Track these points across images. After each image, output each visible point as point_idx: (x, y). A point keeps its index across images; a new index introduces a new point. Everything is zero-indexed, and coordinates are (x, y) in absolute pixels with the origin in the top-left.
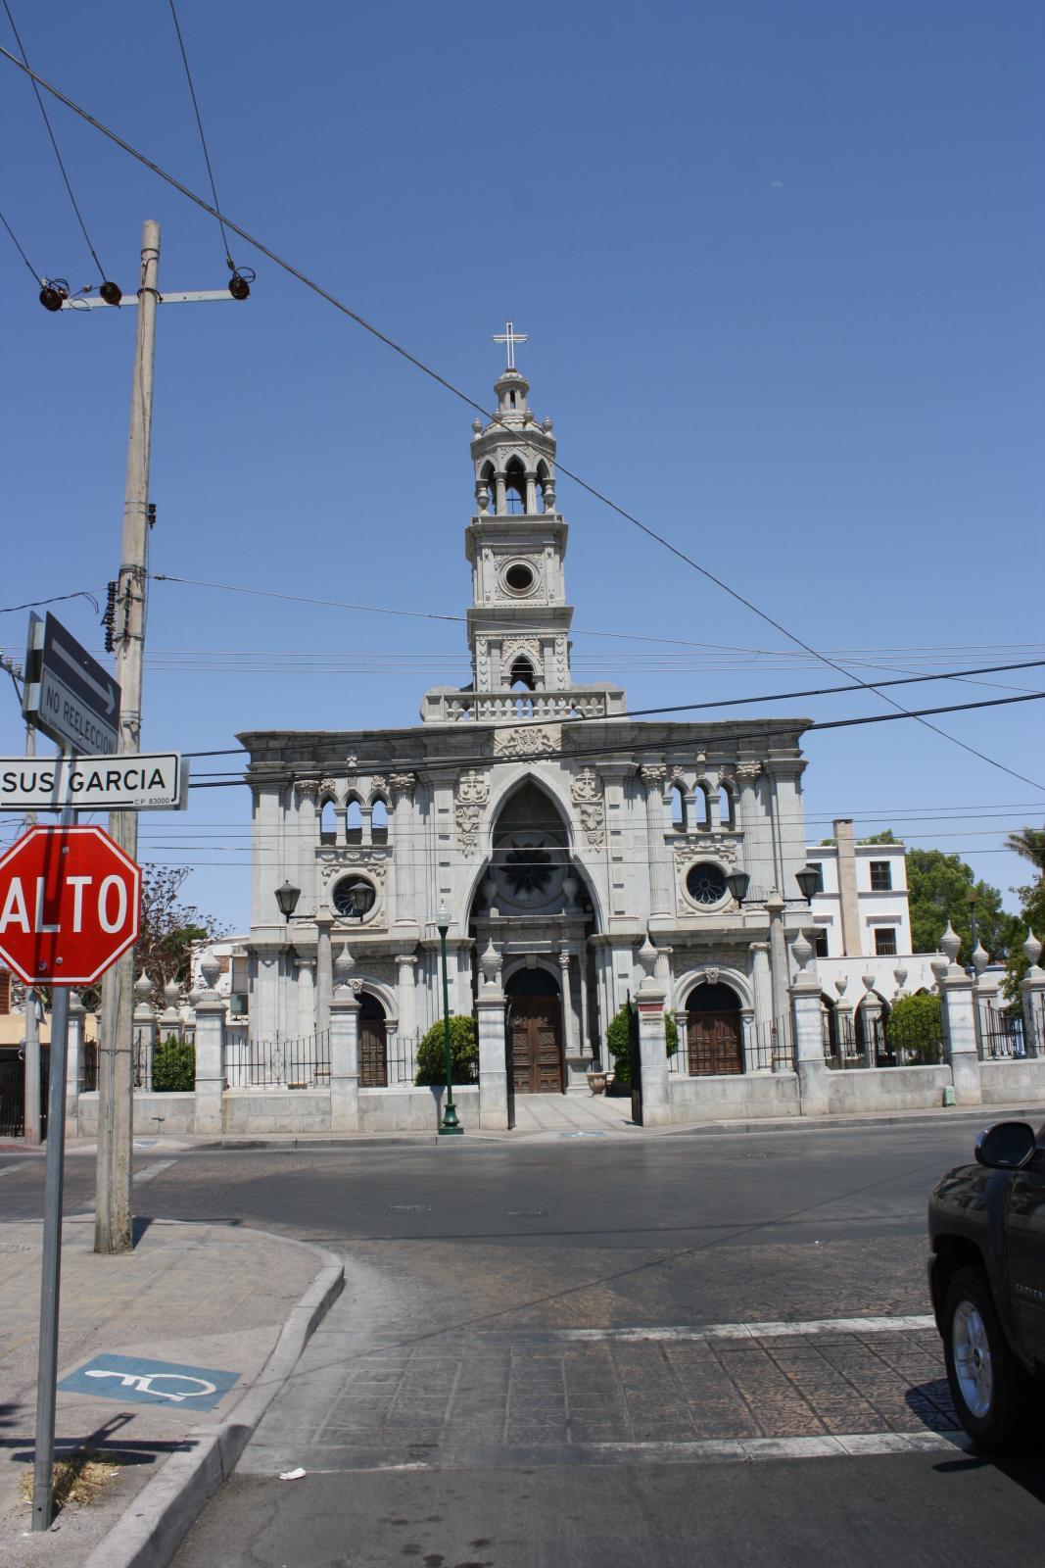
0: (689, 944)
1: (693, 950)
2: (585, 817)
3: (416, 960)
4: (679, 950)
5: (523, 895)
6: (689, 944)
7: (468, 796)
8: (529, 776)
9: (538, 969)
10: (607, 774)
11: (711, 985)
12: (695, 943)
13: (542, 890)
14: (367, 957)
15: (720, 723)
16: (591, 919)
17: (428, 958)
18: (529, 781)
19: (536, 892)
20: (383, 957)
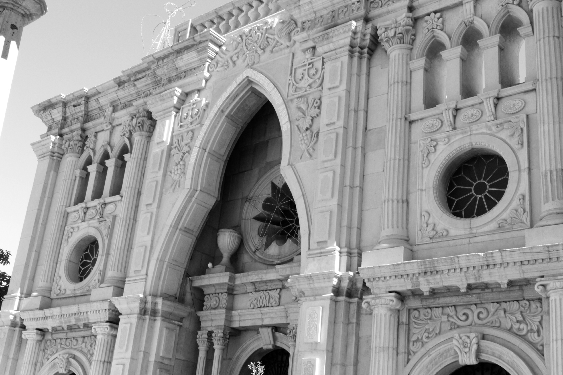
0: (425, 289)
6: (425, 289)
10: (326, 48)
11: (467, 368)
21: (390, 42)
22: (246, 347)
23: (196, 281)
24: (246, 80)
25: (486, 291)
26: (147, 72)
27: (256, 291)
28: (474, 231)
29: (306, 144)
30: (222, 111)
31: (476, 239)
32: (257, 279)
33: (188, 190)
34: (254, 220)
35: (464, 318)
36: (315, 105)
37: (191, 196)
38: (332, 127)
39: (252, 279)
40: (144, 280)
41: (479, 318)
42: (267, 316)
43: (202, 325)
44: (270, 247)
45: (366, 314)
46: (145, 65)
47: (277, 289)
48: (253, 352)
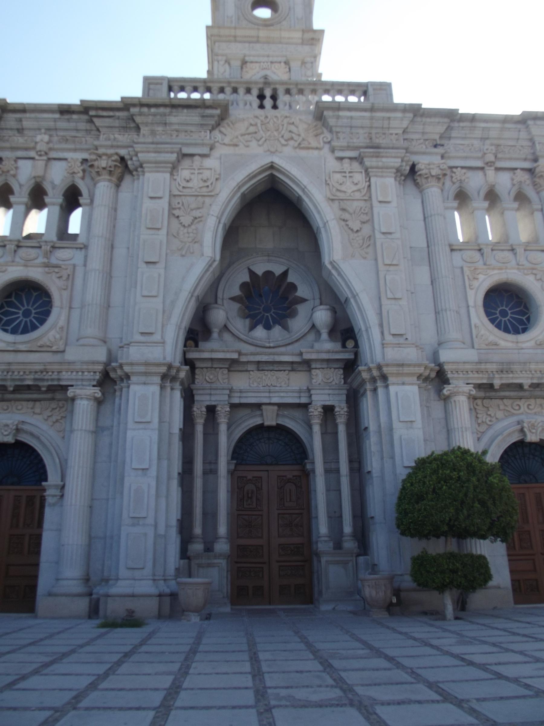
1: (502, 394)
2: (346, 216)
3: (99, 395)
4: (482, 394)
5: (260, 332)
6: (497, 383)
7: (190, 185)
8: (272, 167)
9: (280, 429)
10: (374, 164)
11: (531, 444)
12: (504, 381)
13: (285, 328)
14: (29, 387)
15: (513, 116)
16: (352, 357)
17: (118, 393)
18: (272, 177)
19: (277, 330)
20: (51, 389)
21: (429, 180)
22: (240, 424)
23: (191, 353)
24: (270, 165)
25: (537, 389)
26: (118, 114)
27: (258, 370)
28: (520, 345)
29: (359, 244)
30: (239, 188)
31: (523, 351)
32: (268, 359)
33: (210, 258)
34: (231, 301)
35: (517, 408)
36: (362, 210)
37: (210, 266)
38: (389, 236)
39: (262, 359)
40: (161, 345)
41: (528, 408)
42: (277, 394)
43: (197, 398)
44: (255, 329)
45: (435, 400)
46: (121, 105)
47: (284, 371)
48: (248, 428)
